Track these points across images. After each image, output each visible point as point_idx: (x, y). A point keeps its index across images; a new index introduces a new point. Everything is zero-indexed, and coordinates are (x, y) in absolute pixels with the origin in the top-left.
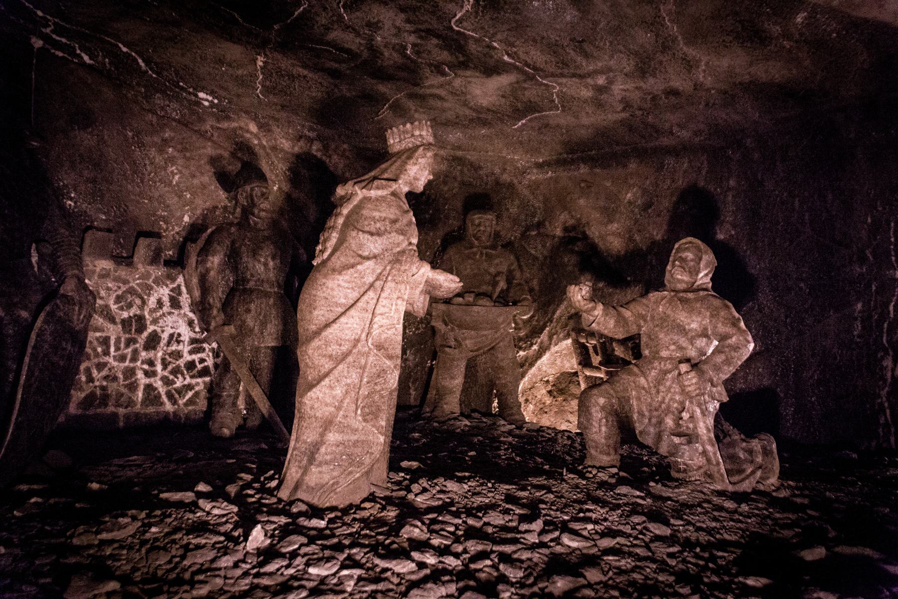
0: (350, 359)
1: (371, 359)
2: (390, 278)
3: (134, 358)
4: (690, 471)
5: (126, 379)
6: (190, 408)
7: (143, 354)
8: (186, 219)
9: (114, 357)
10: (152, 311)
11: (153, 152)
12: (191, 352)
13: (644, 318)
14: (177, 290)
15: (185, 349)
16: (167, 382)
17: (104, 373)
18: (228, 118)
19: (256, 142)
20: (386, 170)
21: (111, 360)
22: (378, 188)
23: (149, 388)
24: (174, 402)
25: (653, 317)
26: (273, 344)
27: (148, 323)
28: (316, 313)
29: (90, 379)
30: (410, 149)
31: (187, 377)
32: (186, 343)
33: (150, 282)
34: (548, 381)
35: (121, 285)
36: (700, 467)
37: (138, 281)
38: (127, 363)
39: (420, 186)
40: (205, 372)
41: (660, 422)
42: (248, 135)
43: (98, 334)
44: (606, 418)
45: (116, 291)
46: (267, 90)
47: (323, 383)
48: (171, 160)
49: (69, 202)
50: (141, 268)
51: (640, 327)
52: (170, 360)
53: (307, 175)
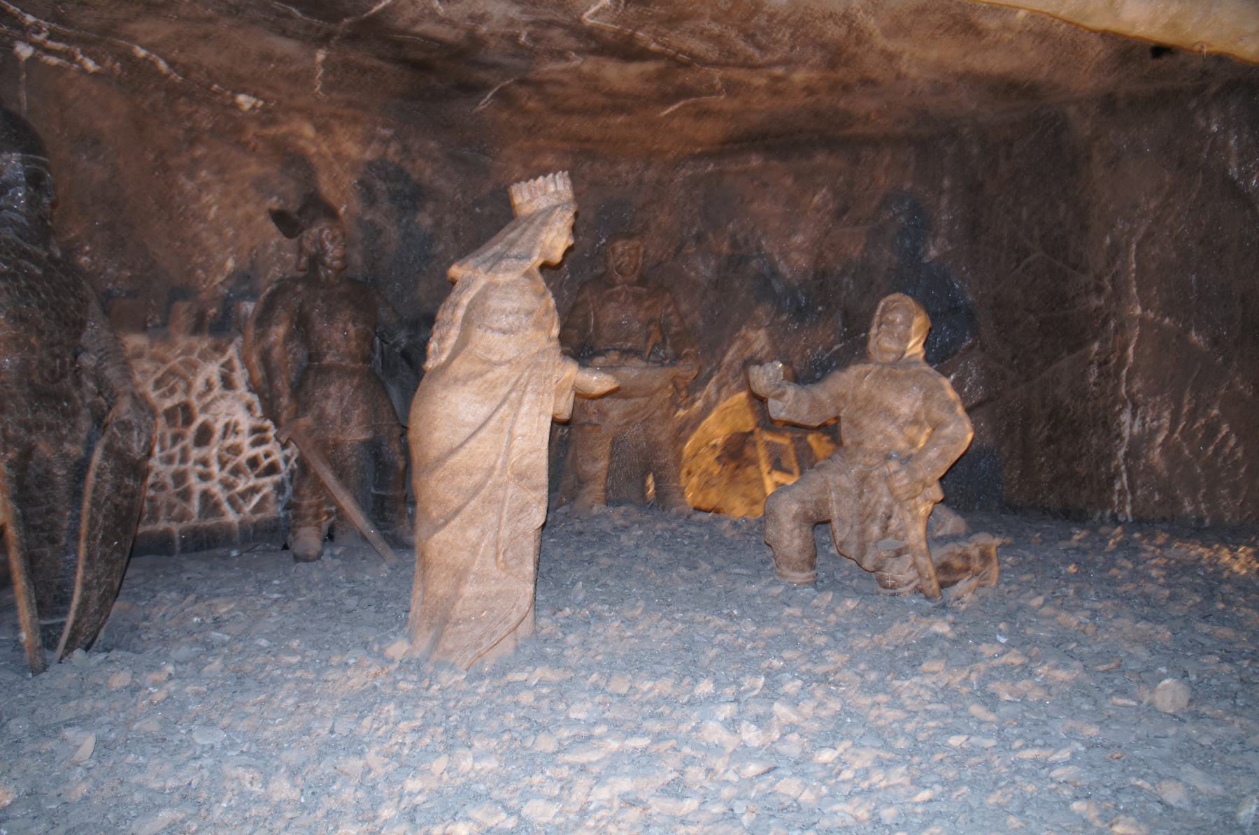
0: (484, 492)
1: (510, 492)
2: (529, 388)
3: (184, 460)
4: (899, 586)
6: (259, 516)
7: (195, 453)
8: (230, 264)
9: (161, 459)
10: (201, 396)
11: (182, 179)
12: (256, 444)
13: (843, 397)
14: (228, 365)
15: (245, 440)
16: (228, 486)
18: (273, 121)
19: (313, 150)
20: (512, 244)
22: (507, 270)
23: (206, 495)
24: (238, 511)
25: (854, 398)
26: (363, 437)
27: (197, 410)
28: (437, 435)
30: (544, 211)
31: (252, 476)
32: (246, 432)
33: (195, 357)
34: (715, 446)
35: (160, 364)
36: (911, 582)
37: (181, 358)
38: (175, 466)
39: (557, 256)
40: (272, 469)
41: (863, 532)
42: (302, 143)
44: (800, 526)
45: (155, 372)
46: (328, 88)
47: (453, 523)
48: (205, 186)
50: (182, 341)
51: (839, 410)
52: (229, 456)
53: (384, 188)
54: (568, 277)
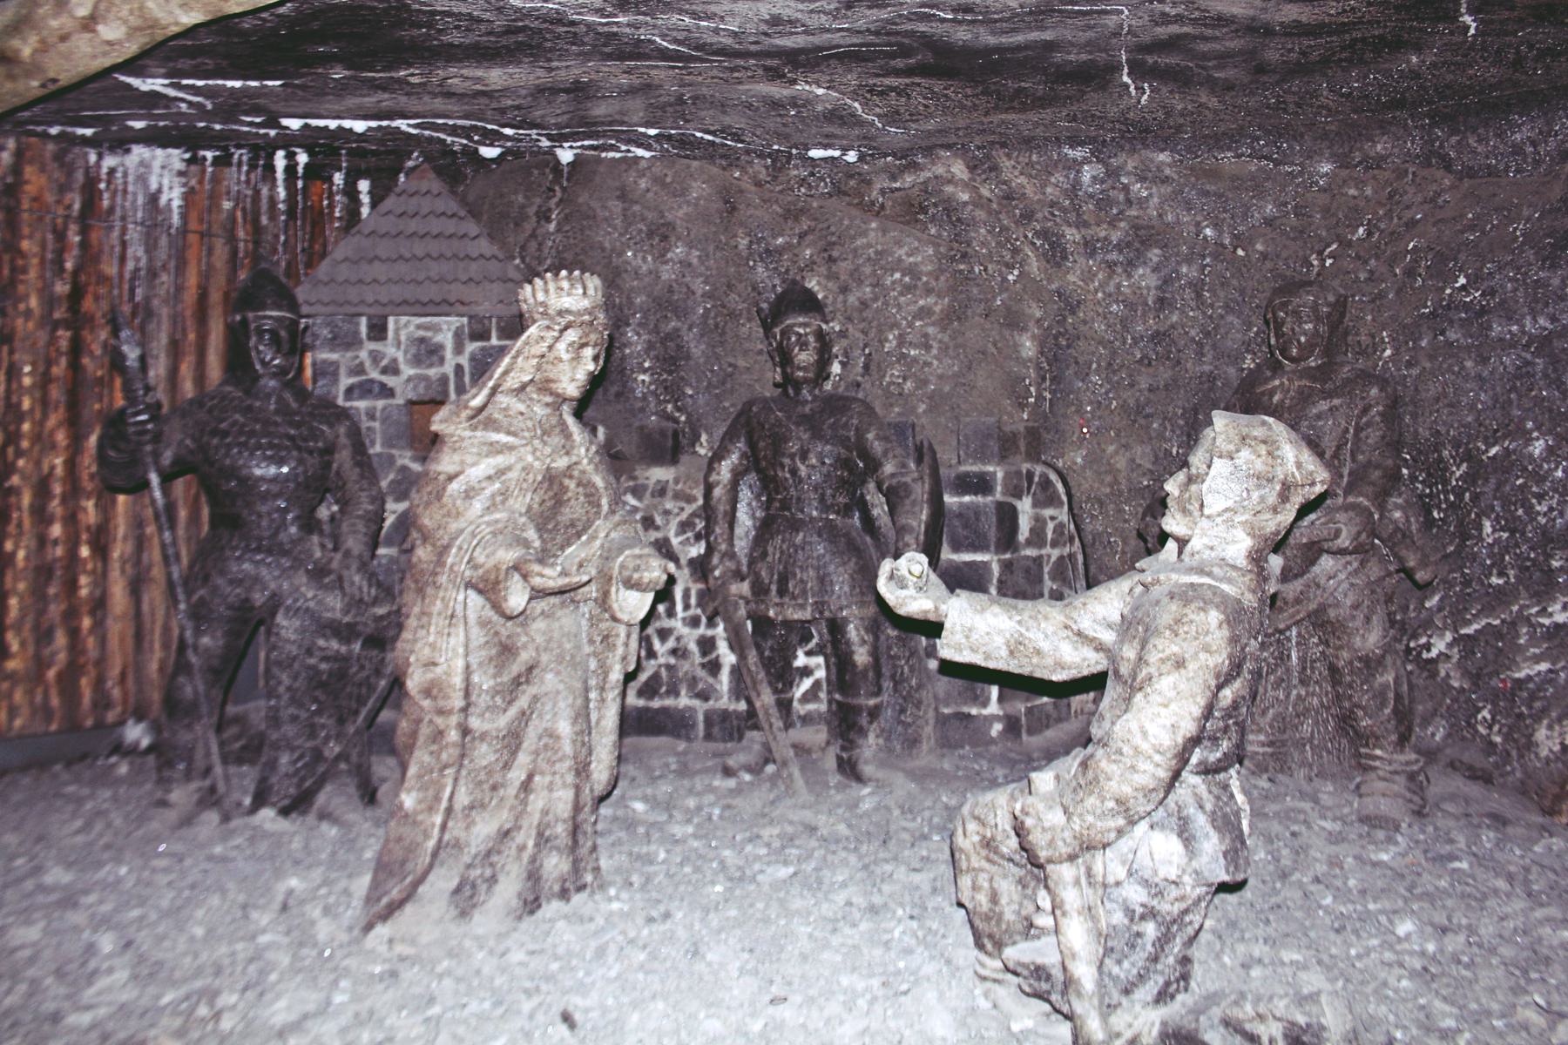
5: (704, 653)
9: (684, 619)
17: (671, 643)
19: (965, 197)
35: (683, 504)
42: (949, 189)
49: (642, 377)
54: (1388, 352)
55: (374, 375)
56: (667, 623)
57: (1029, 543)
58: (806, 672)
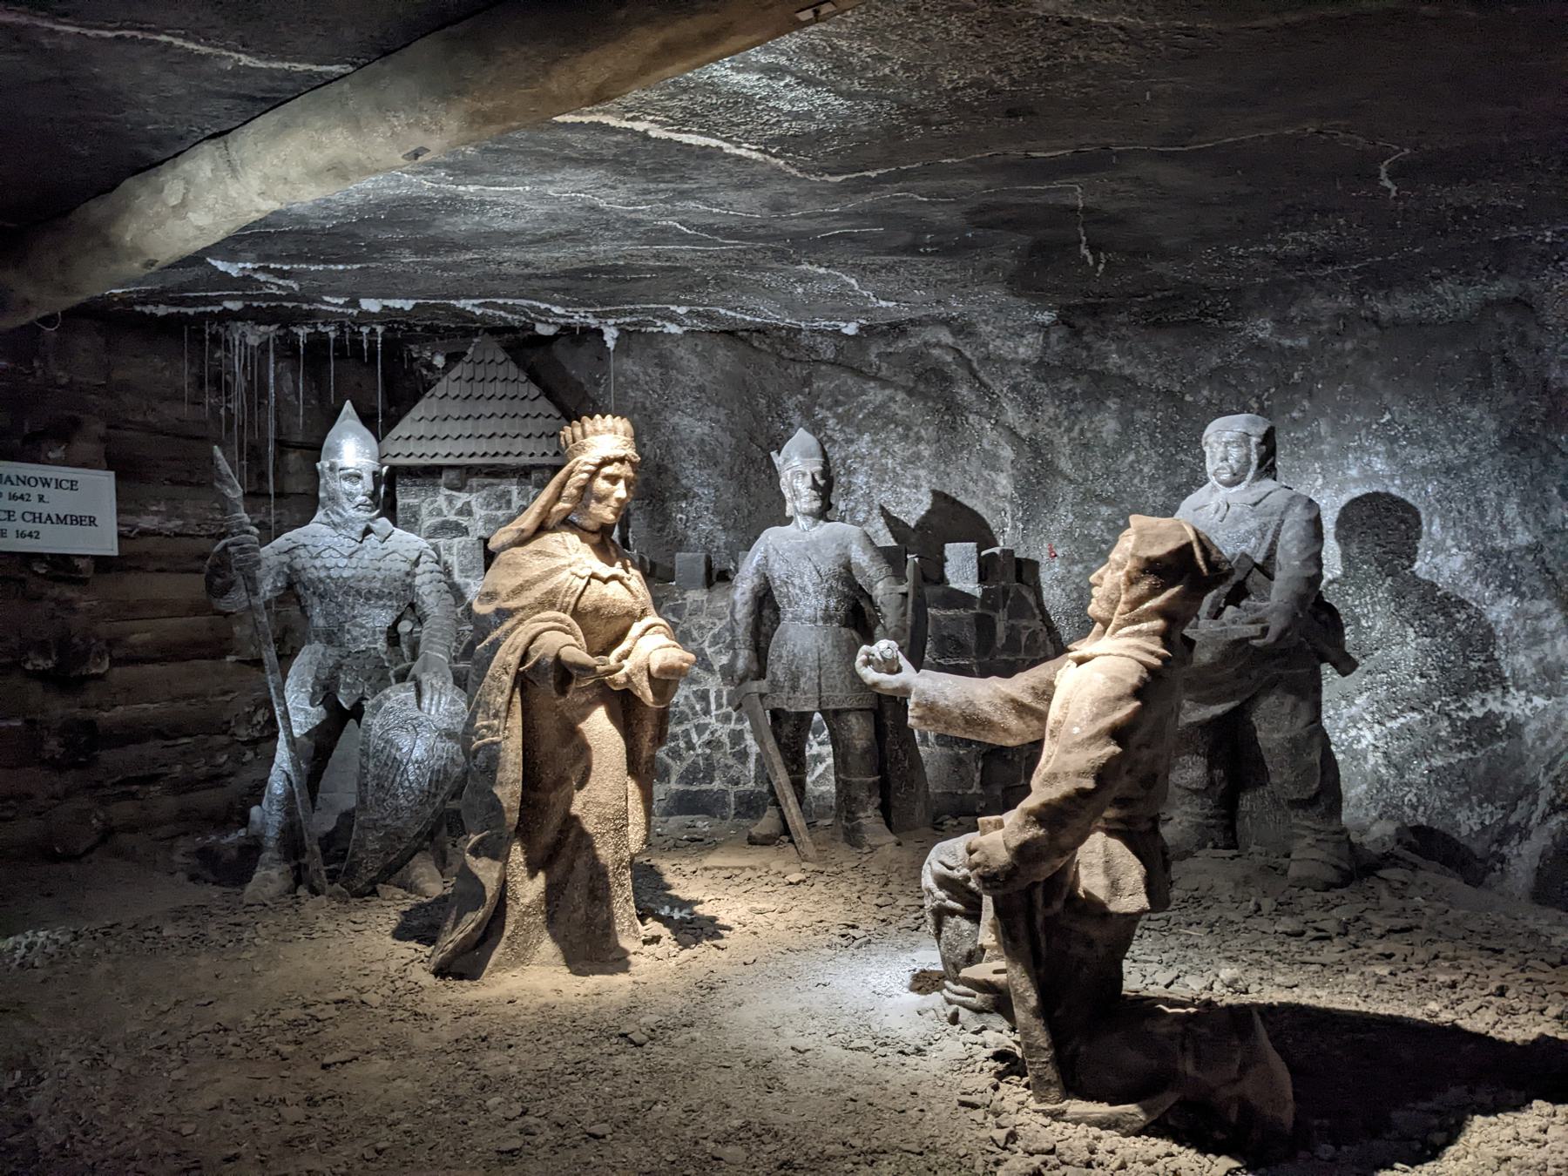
17: (706, 736)
21: (713, 721)
29: (690, 746)
38: (732, 725)
42: (936, 352)
43: (695, 687)
49: (680, 516)
55: (452, 518)
56: (706, 720)
57: (1004, 649)
58: (819, 758)
